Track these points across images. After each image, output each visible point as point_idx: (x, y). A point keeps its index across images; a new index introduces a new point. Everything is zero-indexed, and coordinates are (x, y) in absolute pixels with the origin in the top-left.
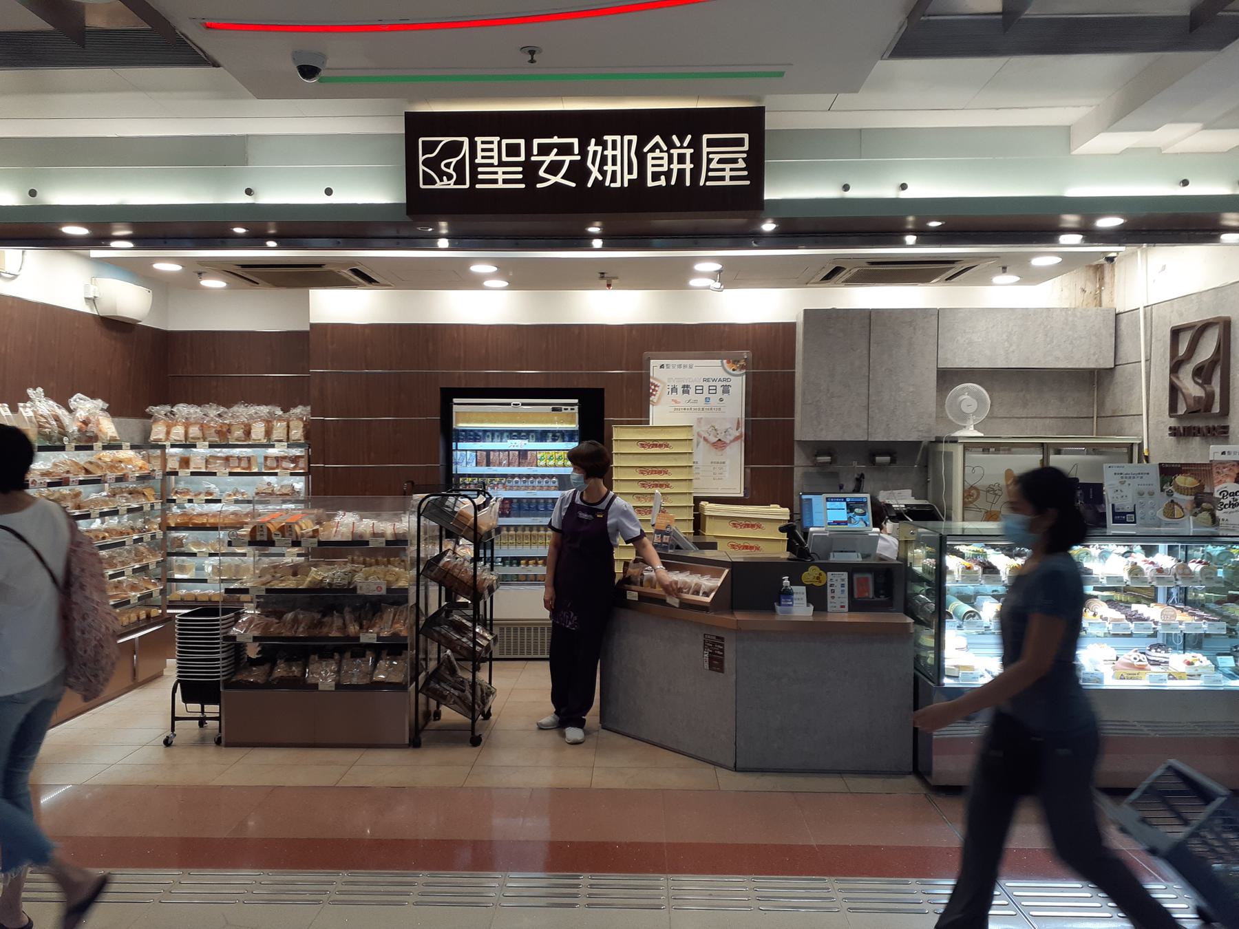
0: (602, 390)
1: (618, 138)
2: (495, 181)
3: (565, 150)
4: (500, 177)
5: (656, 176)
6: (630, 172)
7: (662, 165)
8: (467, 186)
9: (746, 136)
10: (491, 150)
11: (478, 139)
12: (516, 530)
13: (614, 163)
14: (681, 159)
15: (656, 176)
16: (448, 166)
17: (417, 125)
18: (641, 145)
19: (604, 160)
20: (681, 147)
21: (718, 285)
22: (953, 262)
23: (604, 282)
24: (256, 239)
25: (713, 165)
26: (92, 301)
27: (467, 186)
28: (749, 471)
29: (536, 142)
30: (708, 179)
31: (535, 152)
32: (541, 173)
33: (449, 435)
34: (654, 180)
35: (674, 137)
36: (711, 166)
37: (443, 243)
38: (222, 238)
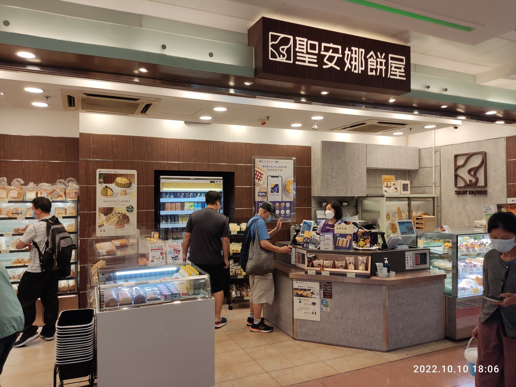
1: (357, 49)
2: (304, 61)
3: (336, 51)
5: (372, 70)
6: (362, 66)
10: (303, 45)
11: (298, 38)
13: (356, 61)
14: (381, 64)
18: (366, 54)
19: (351, 58)
20: (381, 58)
22: (404, 124)
25: (393, 69)
27: (292, 62)
30: (391, 75)
31: (323, 49)
35: (378, 53)
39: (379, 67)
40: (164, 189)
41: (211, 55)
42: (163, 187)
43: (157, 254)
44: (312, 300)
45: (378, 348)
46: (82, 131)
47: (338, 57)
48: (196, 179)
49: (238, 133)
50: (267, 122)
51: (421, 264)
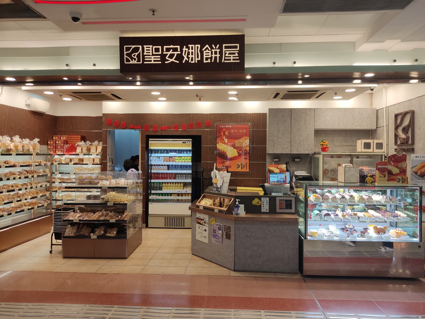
1: (193, 46)
2: (151, 61)
3: (175, 50)
4: (153, 59)
5: (207, 59)
6: (198, 58)
7: (209, 55)
8: (141, 63)
9: (238, 45)
10: (149, 50)
11: (145, 46)
12: (176, 184)
13: (192, 54)
15: (207, 59)
16: (134, 55)
17: (123, 41)
18: (202, 48)
20: (216, 49)
21: (236, 99)
23: (198, 98)
25: (227, 55)
26: (28, 105)
27: (141, 63)
29: (165, 47)
30: (225, 60)
31: (165, 50)
32: (167, 58)
34: (206, 60)
35: (213, 45)
36: (226, 55)
37: (138, 83)
39: (214, 56)
40: (151, 148)
41: (94, 65)
44: (205, 228)
46: (104, 112)
47: (177, 54)
48: (173, 141)
49: (205, 107)
50: (202, 98)
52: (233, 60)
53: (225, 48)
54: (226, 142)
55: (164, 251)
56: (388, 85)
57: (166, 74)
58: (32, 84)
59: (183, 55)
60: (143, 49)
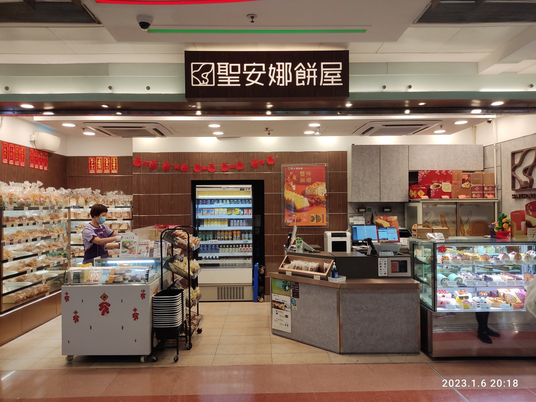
0: (263, 181)
1: (283, 64)
3: (259, 69)
5: (300, 81)
6: (289, 79)
7: (303, 76)
9: (340, 64)
10: (225, 69)
11: (219, 64)
13: (281, 75)
16: (205, 76)
17: (190, 57)
20: (312, 68)
23: (267, 132)
24: (112, 111)
25: (326, 76)
26: (34, 142)
27: (214, 85)
28: (328, 217)
29: (245, 65)
30: (324, 82)
31: (245, 69)
32: (248, 79)
33: (194, 201)
35: (308, 64)
36: (325, 77)
37: (199, 113)
38: (96, 110)
39: (309, 77)
40: (199, 196)
41: (148, 88)
42: (198, 195)
43: (144, 248)
45: (333, 350)
46: (135, 151)
49: (268, 144)
51: (400, 271)
52: (335, 82)
53: (324, 68)
54: (294, 189)
55: (232, 334)
56: (499, 116)
57: (247, 99)
58: (52, 114)
59: (270, 75)
60: (216, 67)
